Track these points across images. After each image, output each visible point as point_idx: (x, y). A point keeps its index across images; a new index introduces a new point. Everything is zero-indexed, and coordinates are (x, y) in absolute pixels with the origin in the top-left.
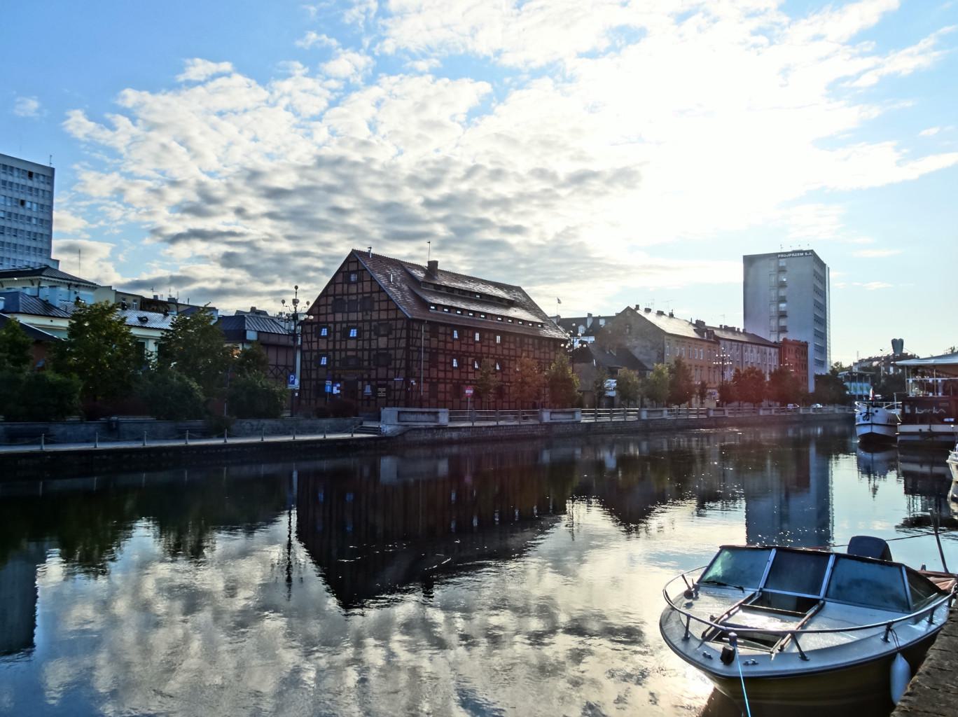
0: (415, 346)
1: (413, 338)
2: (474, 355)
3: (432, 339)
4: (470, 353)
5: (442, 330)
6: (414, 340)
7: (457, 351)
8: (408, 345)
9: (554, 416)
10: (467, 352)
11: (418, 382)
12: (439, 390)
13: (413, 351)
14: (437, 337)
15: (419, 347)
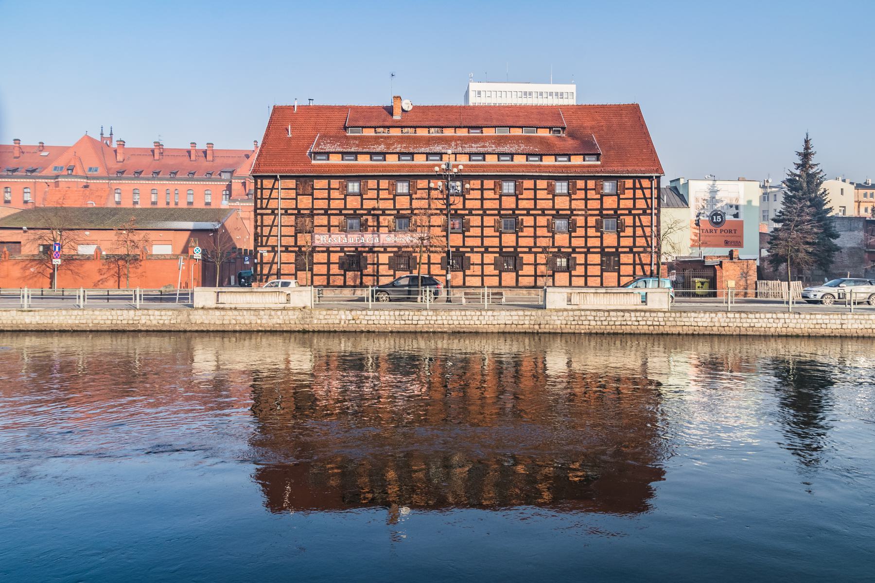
0: (266, 208)
1: (262, 199)
2: (395, 212)
3: (299, 197)
4: (384, 210)
5: (318, 184)
6: (265, 201)
7: (355, 210)
8: (256, 209)
9: (223, 298)
10: (378, 209)
11: (273, 249)
12: (315, 261)
13: (262, 215)
14: (312, 194)
15: (273, 210)
